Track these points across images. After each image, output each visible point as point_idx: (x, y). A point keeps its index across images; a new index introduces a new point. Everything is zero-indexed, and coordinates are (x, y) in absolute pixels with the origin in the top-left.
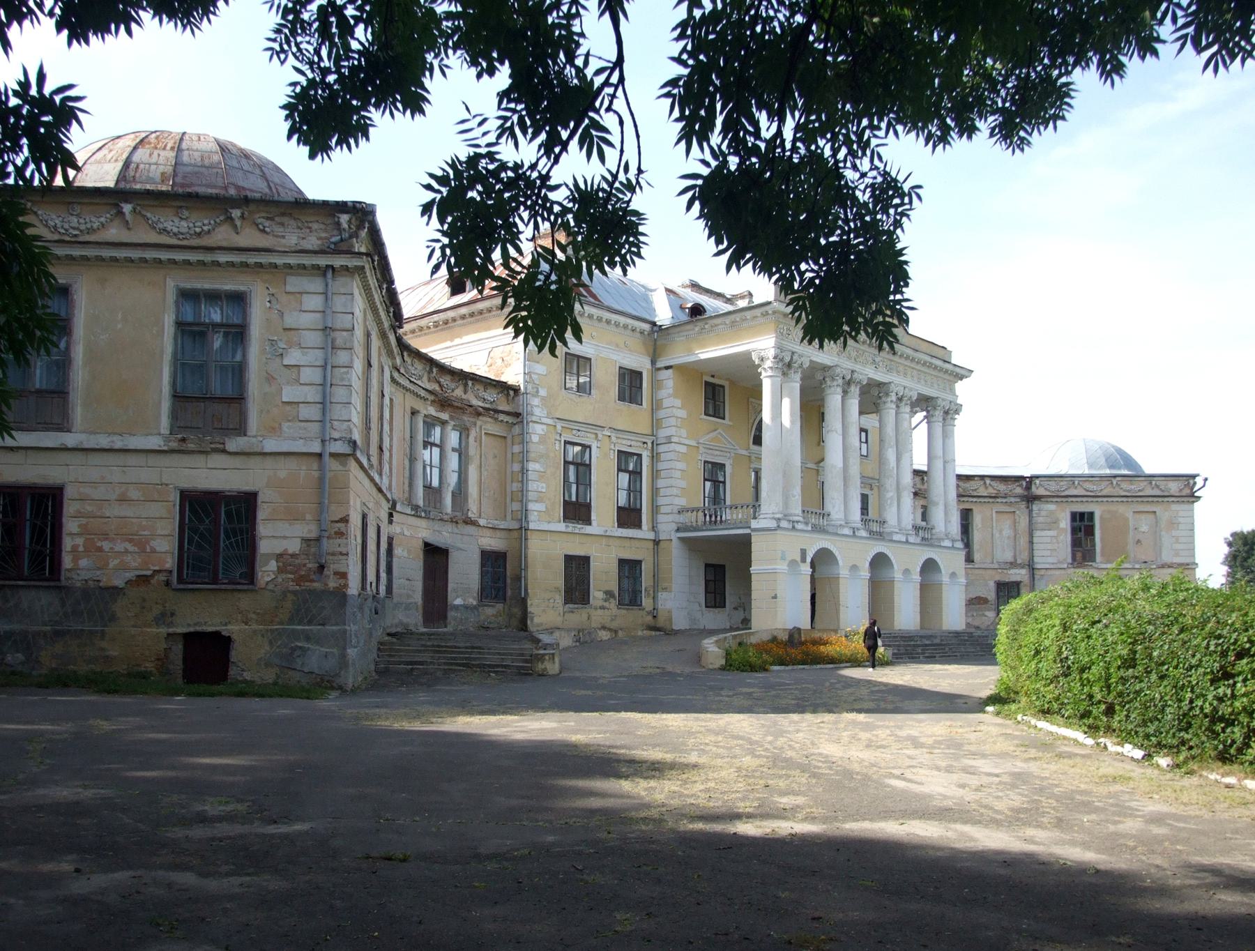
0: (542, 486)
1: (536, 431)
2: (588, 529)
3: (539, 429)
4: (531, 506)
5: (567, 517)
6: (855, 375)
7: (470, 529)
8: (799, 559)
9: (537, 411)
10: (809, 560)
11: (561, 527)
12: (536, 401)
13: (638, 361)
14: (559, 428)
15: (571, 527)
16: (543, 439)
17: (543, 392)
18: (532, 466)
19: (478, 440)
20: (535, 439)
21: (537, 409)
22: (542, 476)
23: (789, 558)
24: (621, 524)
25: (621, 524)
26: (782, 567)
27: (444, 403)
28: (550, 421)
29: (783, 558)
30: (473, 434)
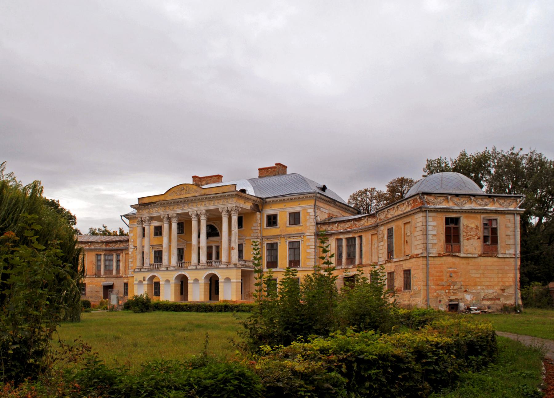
0: (132, 265)
9: (131, 246)
16: (132, 253)
20: (130, 253)
26: (136, 282)
30: (121, 255)
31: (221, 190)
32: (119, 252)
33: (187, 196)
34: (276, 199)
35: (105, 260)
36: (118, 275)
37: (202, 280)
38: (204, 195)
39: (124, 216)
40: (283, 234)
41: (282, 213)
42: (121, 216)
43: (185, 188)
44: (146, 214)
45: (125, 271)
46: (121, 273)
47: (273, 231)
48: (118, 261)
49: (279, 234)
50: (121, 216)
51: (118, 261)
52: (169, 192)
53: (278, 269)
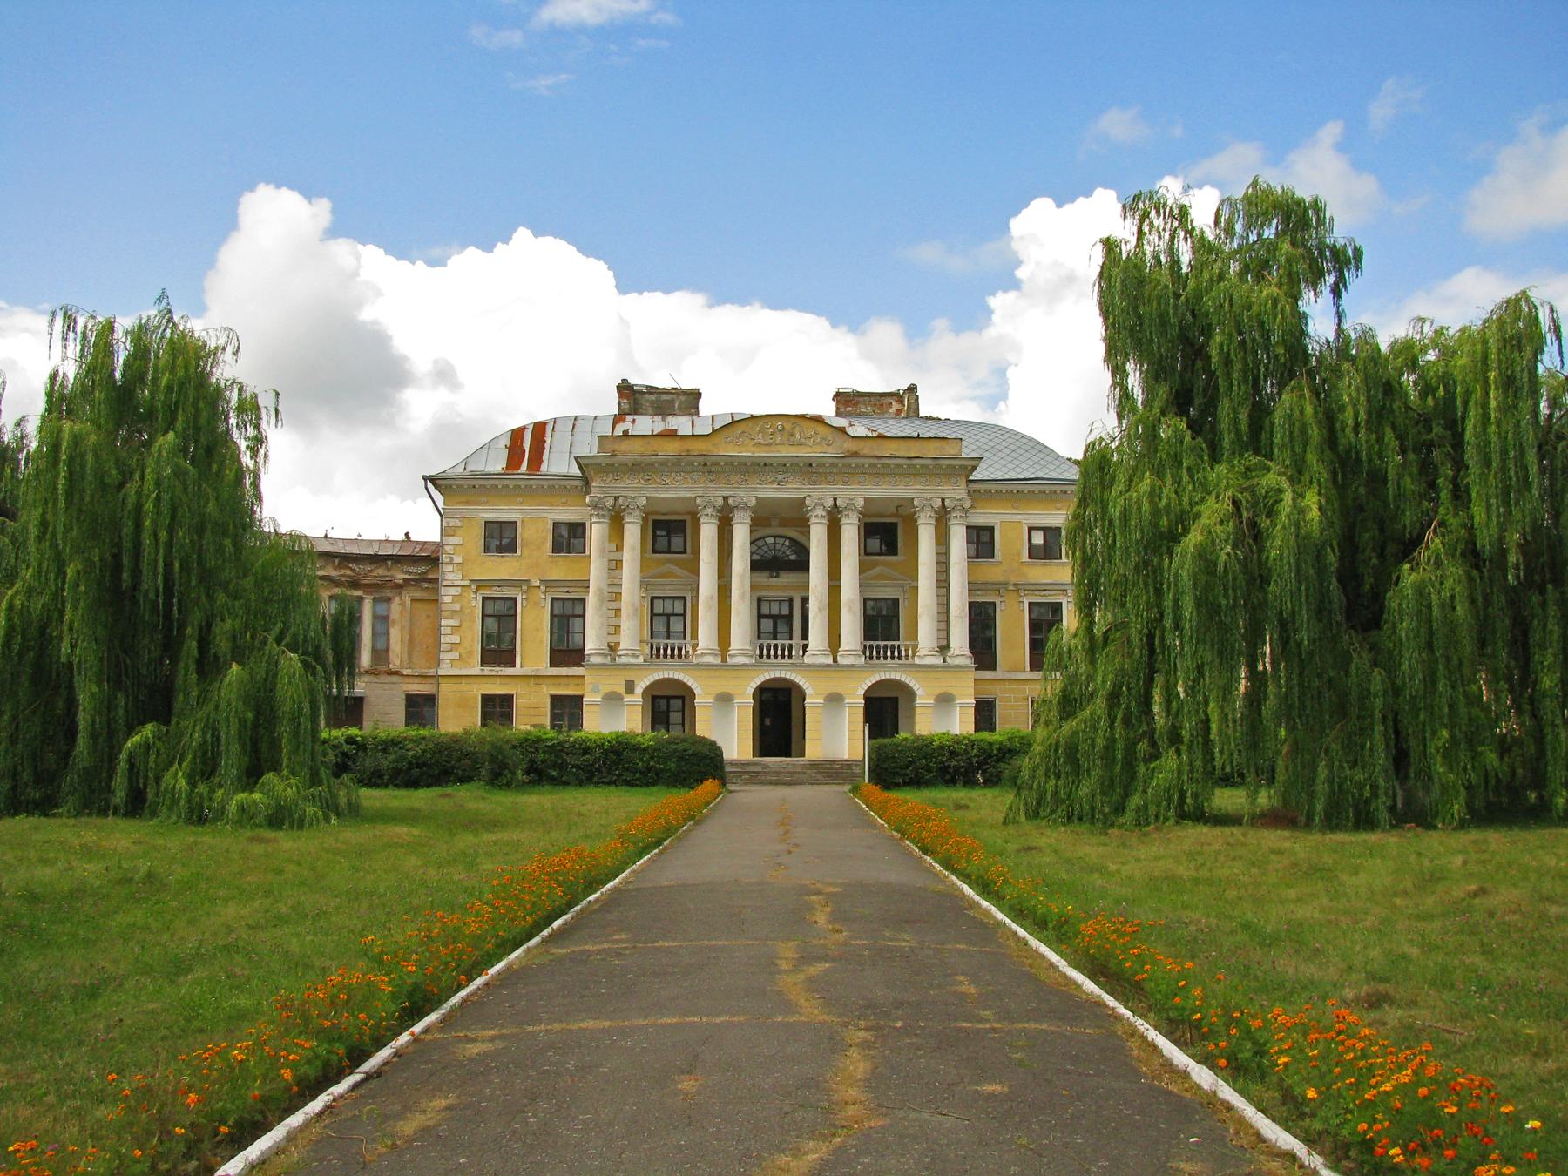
1: (447, 596)
2: (509, 671)
3: (453, 591)
4: (442, 656)
5: (484, 662)
6: (730, 501)
7: (395, 679)
8: (621, 689)
9: (450, 576)
10: (639, 690)
11: (476, 669)
12: (450, 568)
13: (568, 514)
14: (474, 587)
15: (487, 671)
17: (458, 559)
18: (443, 623)
19: (402, 604)
20: (447, 599)
21: (450, 574)
22: (455, 629)
23: (605, 689)
24: (553, 664)
25: (553, 664)
27: (355, 584)
28: (466, 583)
29: (596, 690)
30: (397, 599)
31: (913, 450)
32: (388, 593)
33: (793, 451)
34: (999, 487)
35: (375, 617)
36: (383, 668)
37: (745, 697)
38: (856, 454)
39: (433, 480)
40: (1013, 580)
41: (1015, 527)
42: (425, 478)
43: (788, 426)
44: (638, 493)
45: (410, 656)
46: (396, 659)
47: (991, 571)
48: (382, 621)
49: (1001, 579)
50: (425, 478)
51: (382, 621)
52: (726, 433)
53: (998, 674)
